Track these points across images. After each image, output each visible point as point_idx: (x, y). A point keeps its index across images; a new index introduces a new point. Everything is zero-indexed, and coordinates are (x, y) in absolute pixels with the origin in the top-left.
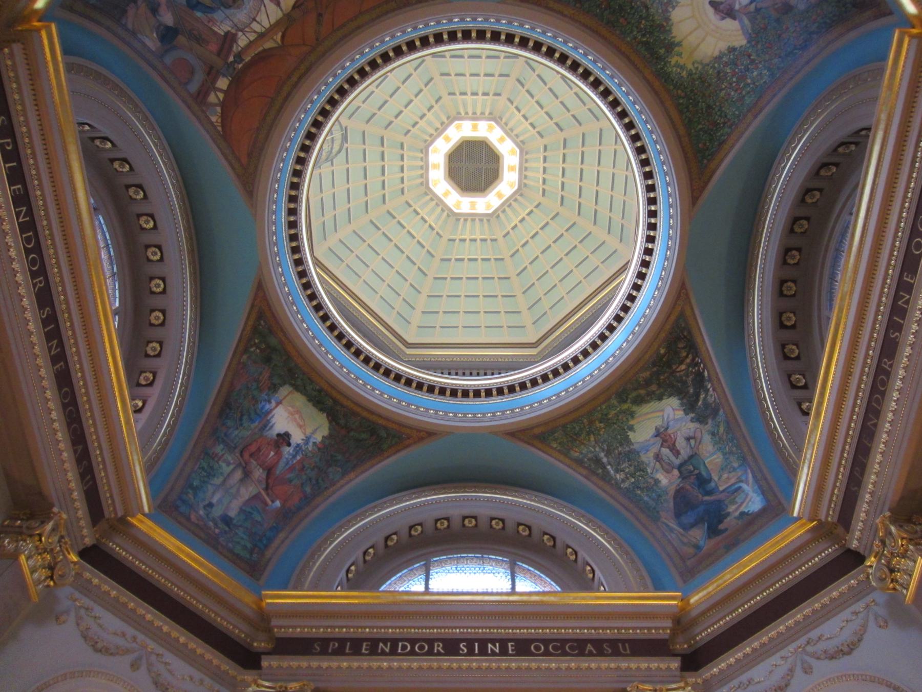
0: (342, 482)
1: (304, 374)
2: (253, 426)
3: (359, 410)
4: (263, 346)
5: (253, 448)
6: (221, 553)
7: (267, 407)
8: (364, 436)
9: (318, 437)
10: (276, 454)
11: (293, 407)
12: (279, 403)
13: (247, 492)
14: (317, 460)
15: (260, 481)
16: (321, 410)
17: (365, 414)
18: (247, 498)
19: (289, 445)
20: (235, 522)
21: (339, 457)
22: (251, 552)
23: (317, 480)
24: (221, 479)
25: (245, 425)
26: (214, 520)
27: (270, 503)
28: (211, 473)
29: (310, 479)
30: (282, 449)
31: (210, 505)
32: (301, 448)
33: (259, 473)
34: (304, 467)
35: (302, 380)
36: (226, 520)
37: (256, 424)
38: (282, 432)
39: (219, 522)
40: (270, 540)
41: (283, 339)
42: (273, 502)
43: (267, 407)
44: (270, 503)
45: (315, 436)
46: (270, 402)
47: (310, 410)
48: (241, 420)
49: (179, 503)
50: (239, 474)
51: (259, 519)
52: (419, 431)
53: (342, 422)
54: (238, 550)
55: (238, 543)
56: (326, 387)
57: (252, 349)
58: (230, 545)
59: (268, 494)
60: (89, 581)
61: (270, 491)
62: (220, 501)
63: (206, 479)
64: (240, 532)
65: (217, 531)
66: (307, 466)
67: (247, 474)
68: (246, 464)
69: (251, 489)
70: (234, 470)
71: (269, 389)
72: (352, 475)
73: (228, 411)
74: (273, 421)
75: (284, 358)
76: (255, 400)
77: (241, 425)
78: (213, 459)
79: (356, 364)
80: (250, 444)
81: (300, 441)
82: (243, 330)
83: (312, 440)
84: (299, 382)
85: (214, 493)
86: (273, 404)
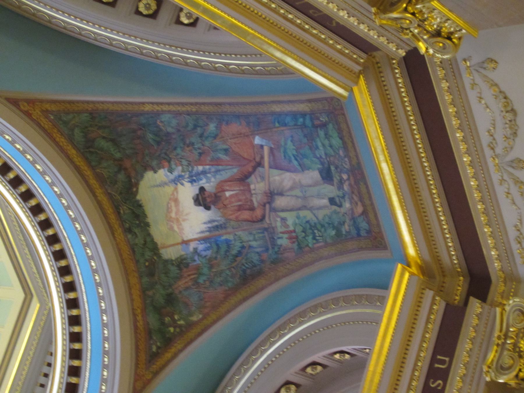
0: (165, 108)
1: (137, 262)
2: (231, 237)
3: (93, 182)
4: (167, 319)
5: (246, 215)
6: (357, 157)
7: (201, 247)
8: (103, 144)
9: (162, 174)
10: (224, 191)
11: (171, 229)
12: (186, 243)
13: (284, 179)
14: (179, 151)
15: (263, 178)
16: (140, 206)
17: (88, 173)
18: (288, 174)
19: (202, 189)
20: (320, 166)
21: (150, 136)
22: (324, 125)
23: (195, 127)
24: (303, 213)
25: (238, 244)
26: (340, 186)
27: (266, 150)
28: (311, 228)
29: (201, 136)
30: (213, 190)
31: (332, 201)
32: (191, 176)
33: (258, 187)
34: (200, 154)
35: (143, 255)
36: (327, 176)
37: (224, 238)
38: (202, 208)
39: (336, 181)
40: (295, 115)
41: (139, 318)
42: (262, 147)
43: (201, 247)
44: (266, 150)
45: (165, 179)
46: (195, 250)
47: (154, 214)
48: (240, 253)
49: (363, 233)
50: (280, 202)
51: (289, 143)
52: (28, 114)
53: (121, 176)
54: (336, 141)
55: (331, 146)
56: (119, 231)
57: (182, 322)
58: (341, 153)
59: (262, 157)
60: (499, 258)
61: (258, 159)
62: (319, 196)
63: (319, 227)
64: (321, 152)
65: (345, 177)
66: (196, 153)
67: (271, 195)
68: (264, 205)
69: (277, 178)
70: (283, 211)
71: (187, 265)
72: (148, 108)
73: (248, 272)
74: (204, 227)
75: (150, 293)
76: (211, 263)
77: (243, 247)
78: (297, 237)
79: (62, 228)
80: (247, 220)
81: (188, 185)
82: (181, 351)
83: (172, 177)
84: (148, 254)
85: (320, 208)
86: (192, 246)
